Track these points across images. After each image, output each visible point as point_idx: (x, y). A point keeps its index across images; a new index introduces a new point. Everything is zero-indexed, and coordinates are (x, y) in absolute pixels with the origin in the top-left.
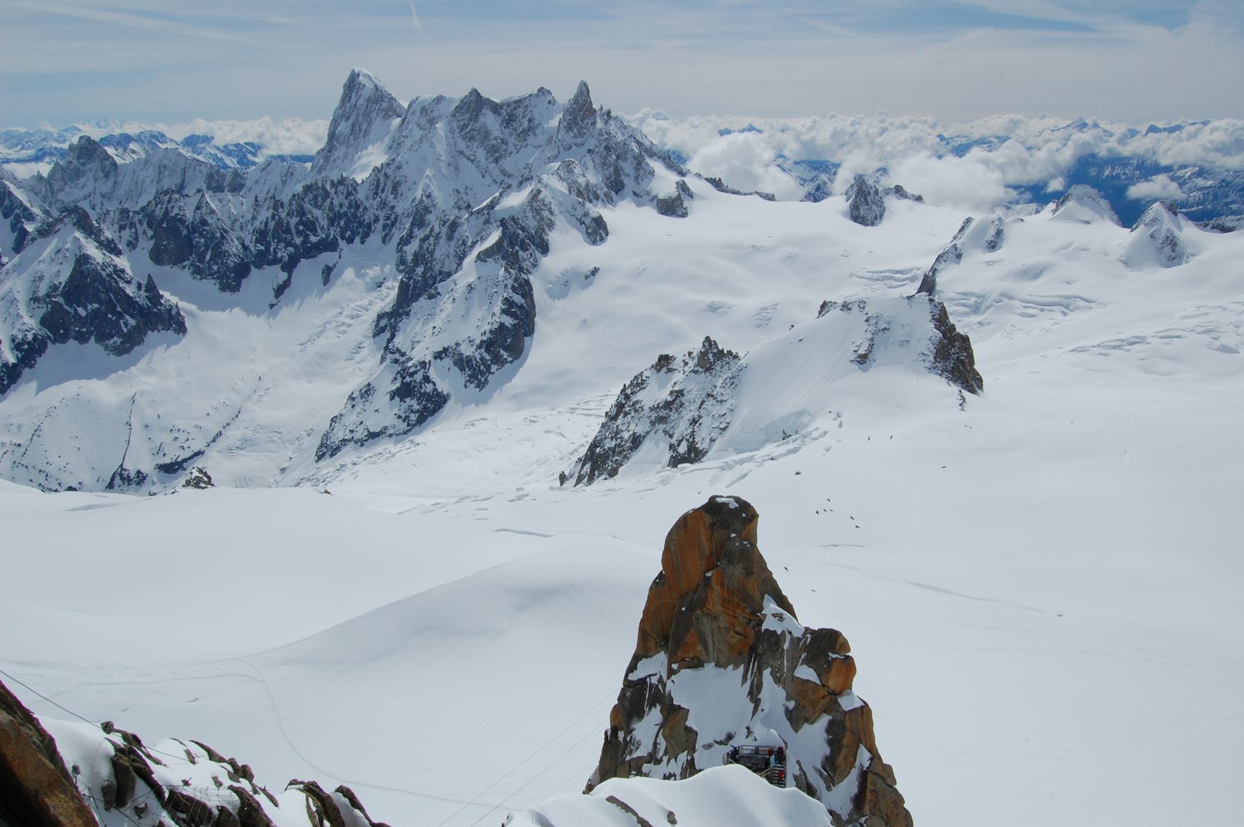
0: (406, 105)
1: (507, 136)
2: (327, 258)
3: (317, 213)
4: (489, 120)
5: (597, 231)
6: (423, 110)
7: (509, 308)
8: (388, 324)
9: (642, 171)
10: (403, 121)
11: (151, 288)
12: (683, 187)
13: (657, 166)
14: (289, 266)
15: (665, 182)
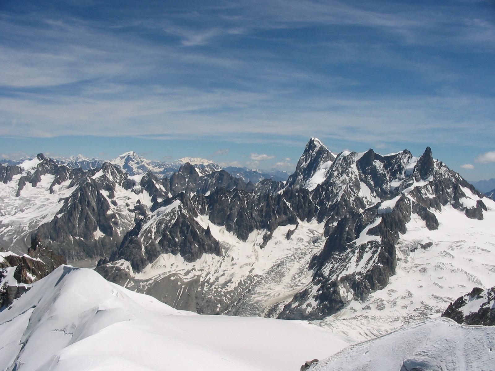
0: (335, 156)
1: (386, 173)
2: (292, 227)
3: (288, 204)
4: (378, 165)
5: (432, 223)
6: (345, 158)
7: (382, 258)
8: (317, 263)
9: (458, 195)
10: (334, 163)
11: (208, 231)
12: (480, 203)
13: (466, 191)
14: (271, 229)
15: (470, 200)
